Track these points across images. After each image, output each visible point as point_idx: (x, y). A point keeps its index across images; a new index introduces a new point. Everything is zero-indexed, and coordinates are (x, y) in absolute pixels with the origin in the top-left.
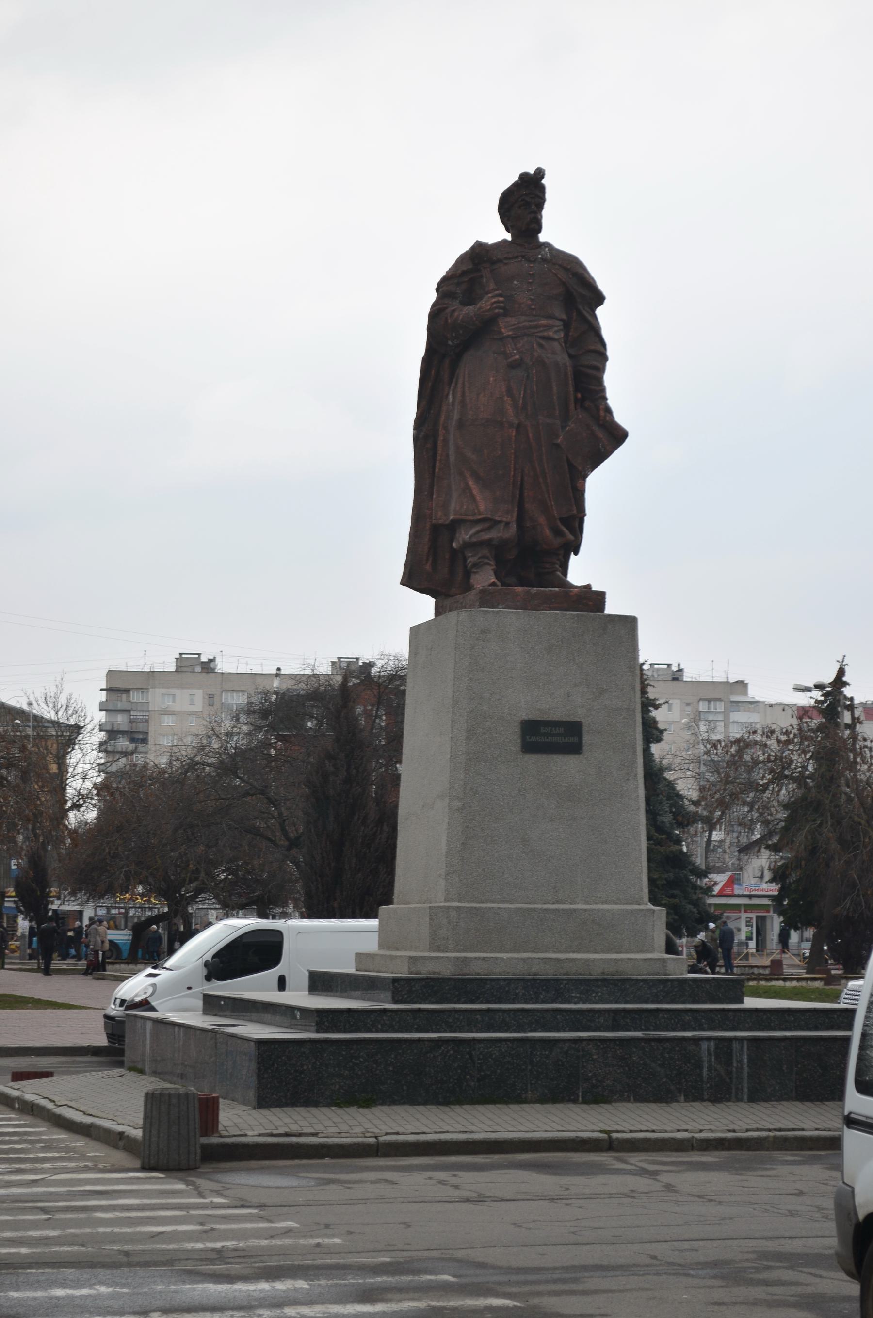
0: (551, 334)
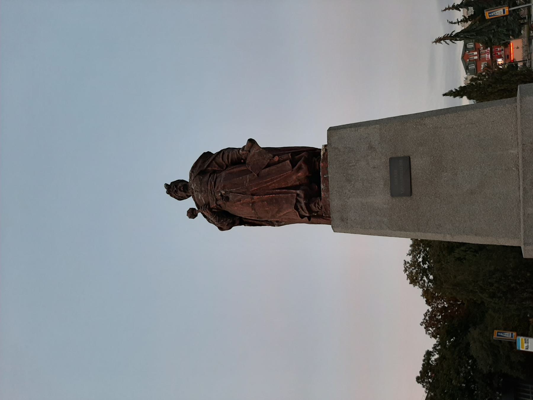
0: (213, 183)
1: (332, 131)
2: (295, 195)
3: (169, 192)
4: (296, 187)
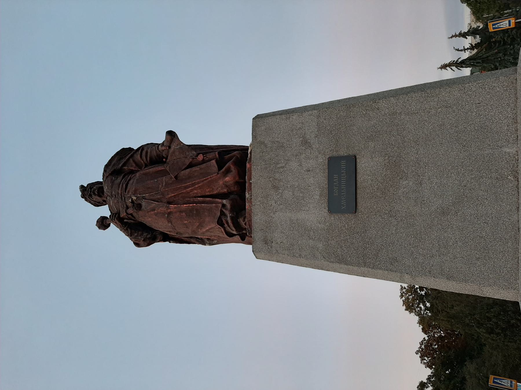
1: (258, 120)
2: (220, 205)
3: (83, 196)
4: (222, 196)
